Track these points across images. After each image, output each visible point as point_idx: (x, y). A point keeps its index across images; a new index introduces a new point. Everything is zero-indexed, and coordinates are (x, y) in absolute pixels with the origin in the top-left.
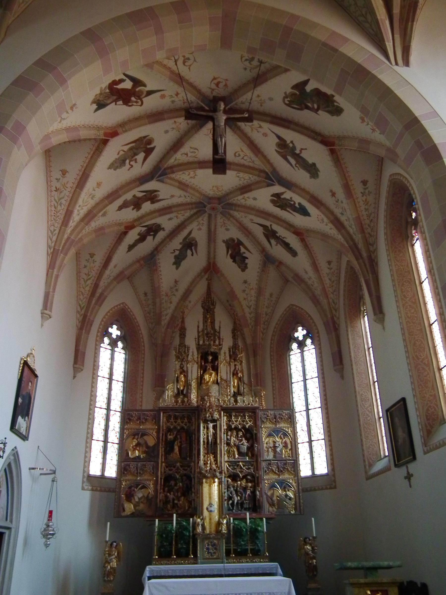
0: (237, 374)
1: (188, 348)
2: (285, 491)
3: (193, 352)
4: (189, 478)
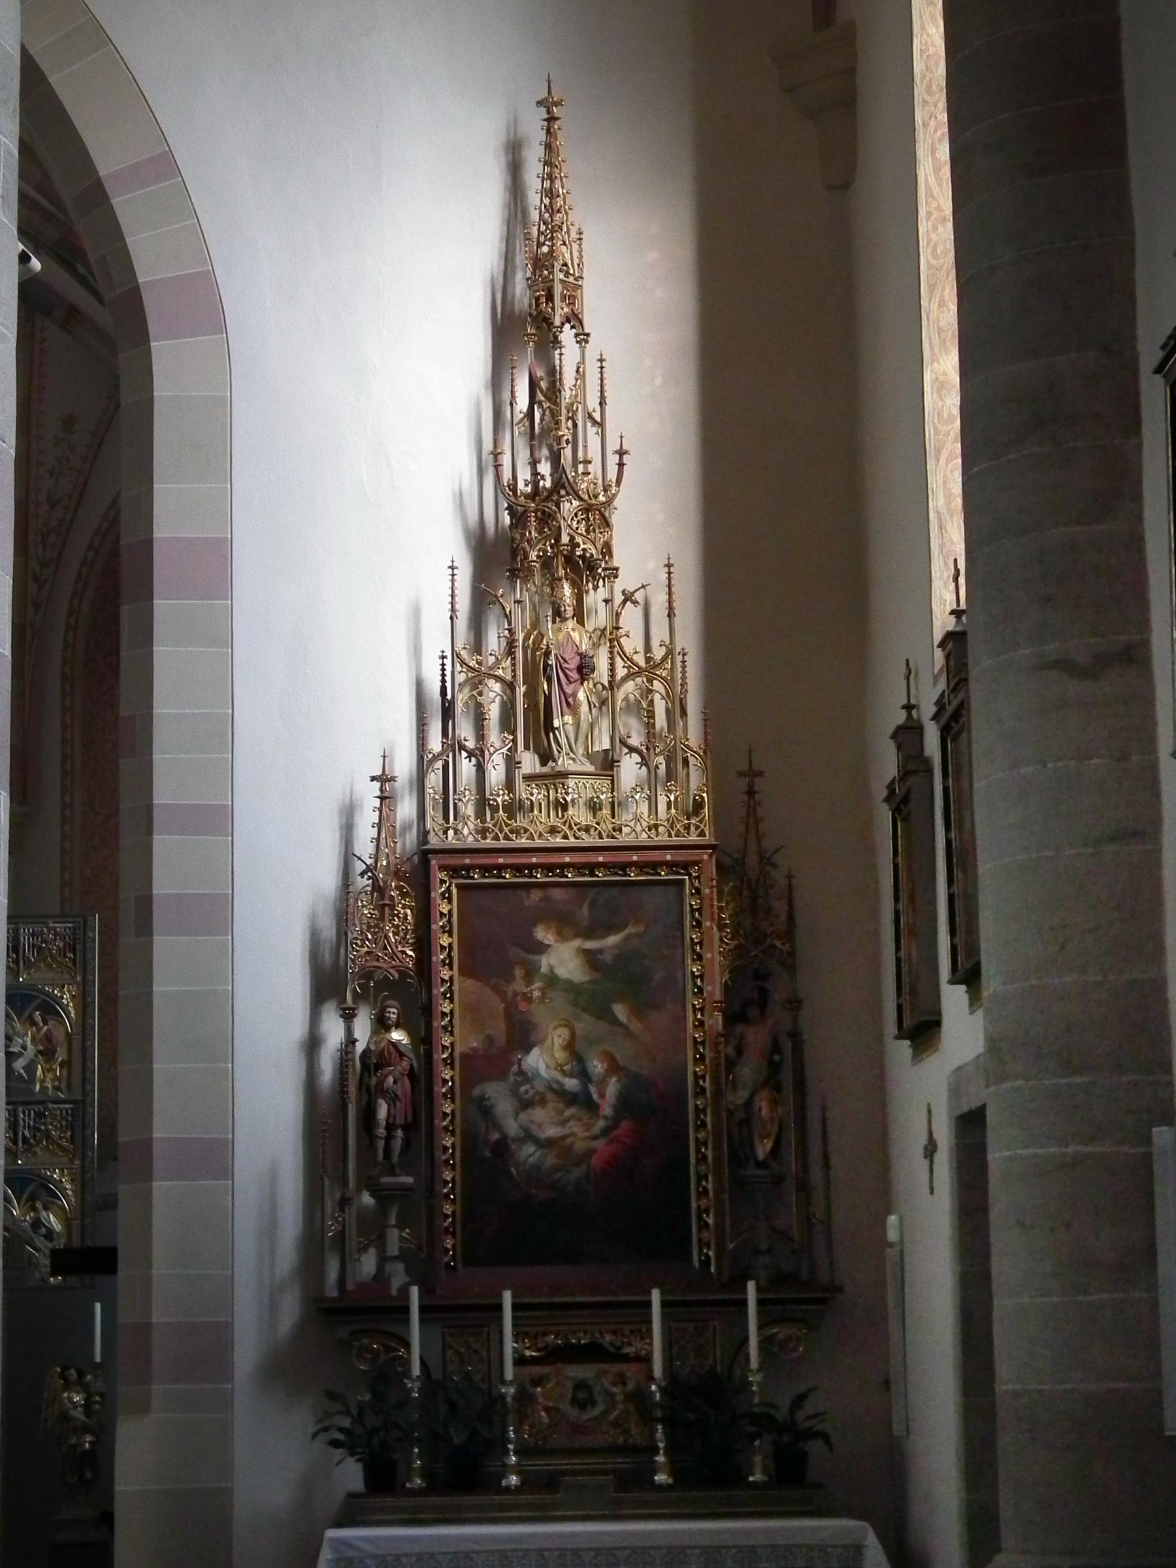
2: (34, 1209)
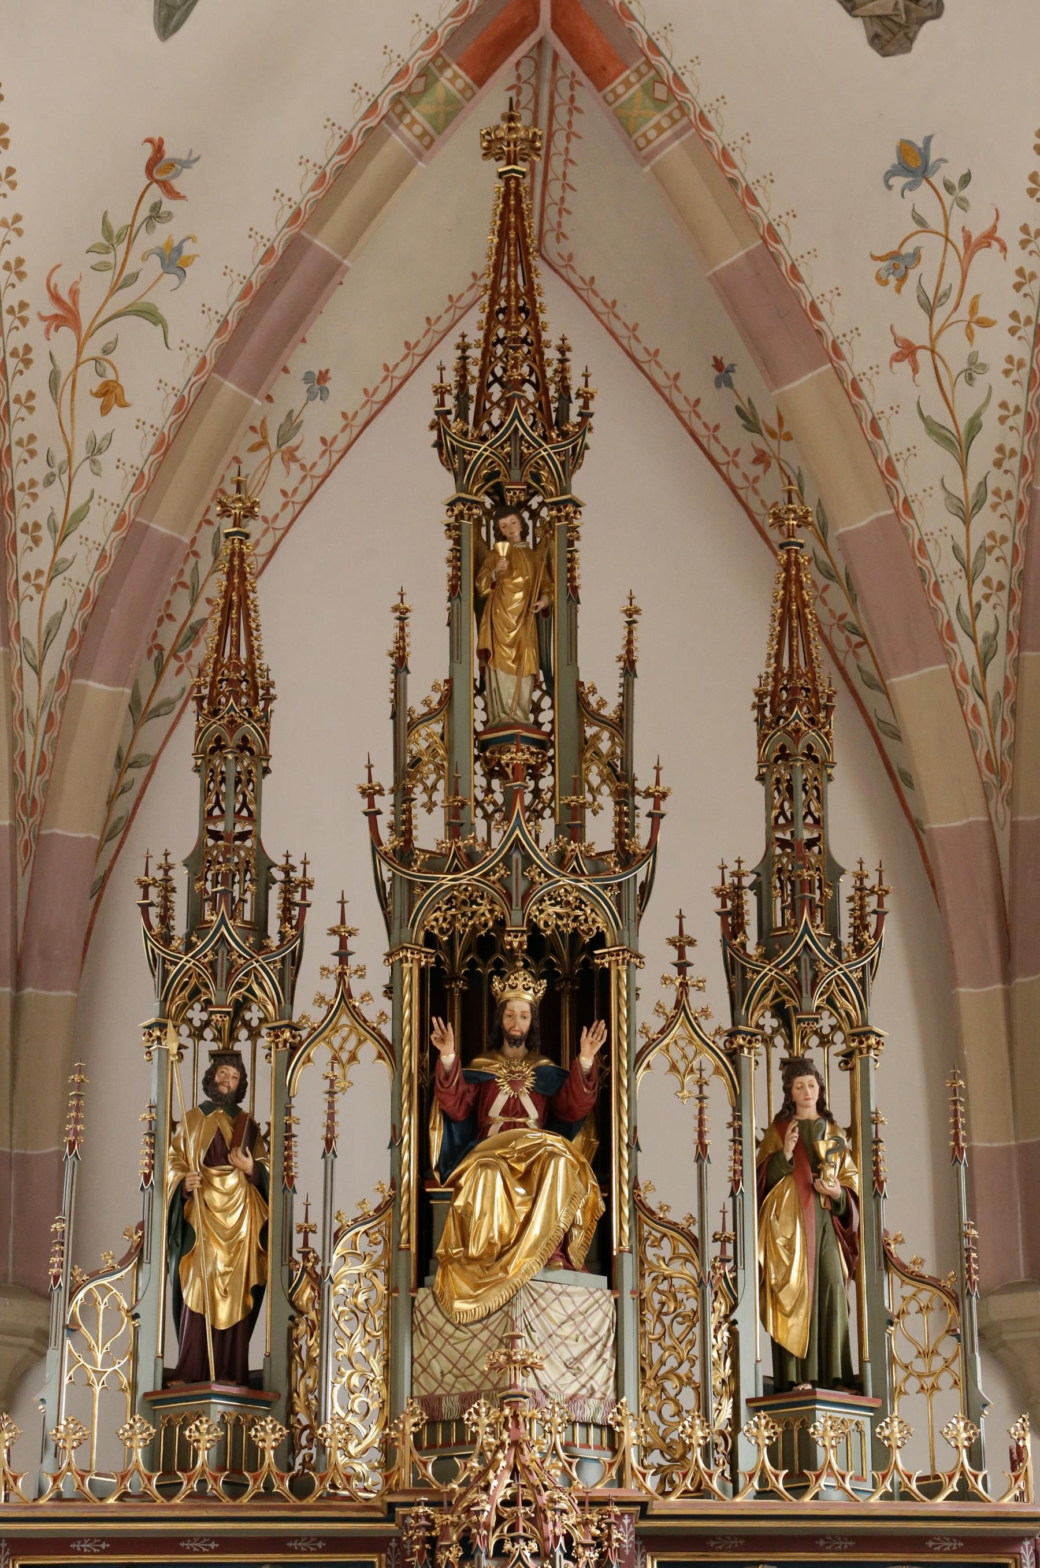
0: (810, 1161)
1: (296, 888)
3: (342, 934)
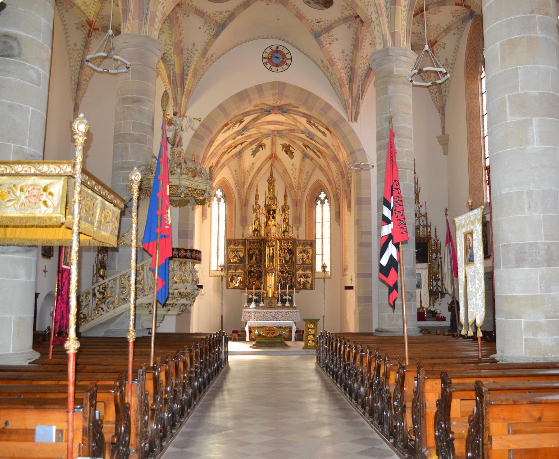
4: (260, 272)
